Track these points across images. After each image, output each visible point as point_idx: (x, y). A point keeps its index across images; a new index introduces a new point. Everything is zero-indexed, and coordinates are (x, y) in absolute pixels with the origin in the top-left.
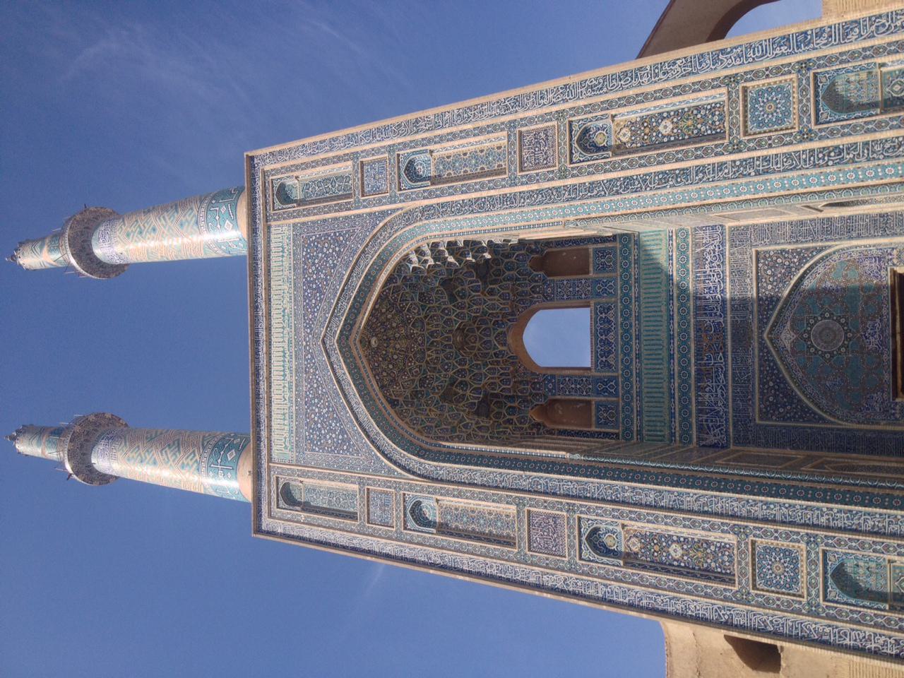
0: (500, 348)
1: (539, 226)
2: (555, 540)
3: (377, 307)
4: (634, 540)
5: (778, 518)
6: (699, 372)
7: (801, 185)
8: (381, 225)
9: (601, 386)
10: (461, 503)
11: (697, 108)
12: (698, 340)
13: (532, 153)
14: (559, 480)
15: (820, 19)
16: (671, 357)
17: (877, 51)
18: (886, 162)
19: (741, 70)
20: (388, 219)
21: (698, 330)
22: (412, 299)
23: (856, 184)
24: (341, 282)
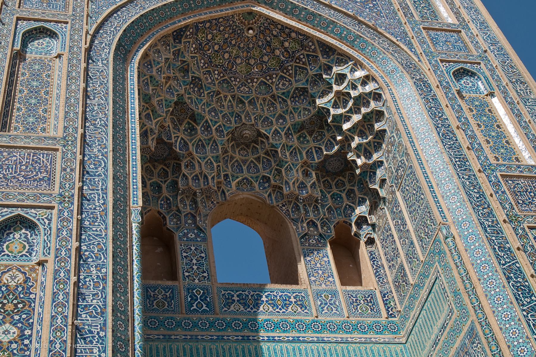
0: (234, 184)
2: (14, 177)
3: (293, 35)
4: (21, 278)
13: (527, 190)
20: (405, 48)
22: (296, 81)
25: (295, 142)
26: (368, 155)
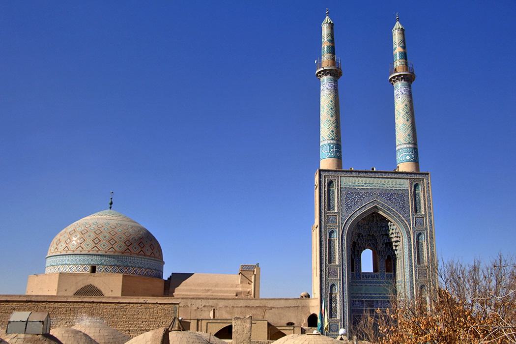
12: (370, 301)
16: (366, 294)
21: (373, 301)
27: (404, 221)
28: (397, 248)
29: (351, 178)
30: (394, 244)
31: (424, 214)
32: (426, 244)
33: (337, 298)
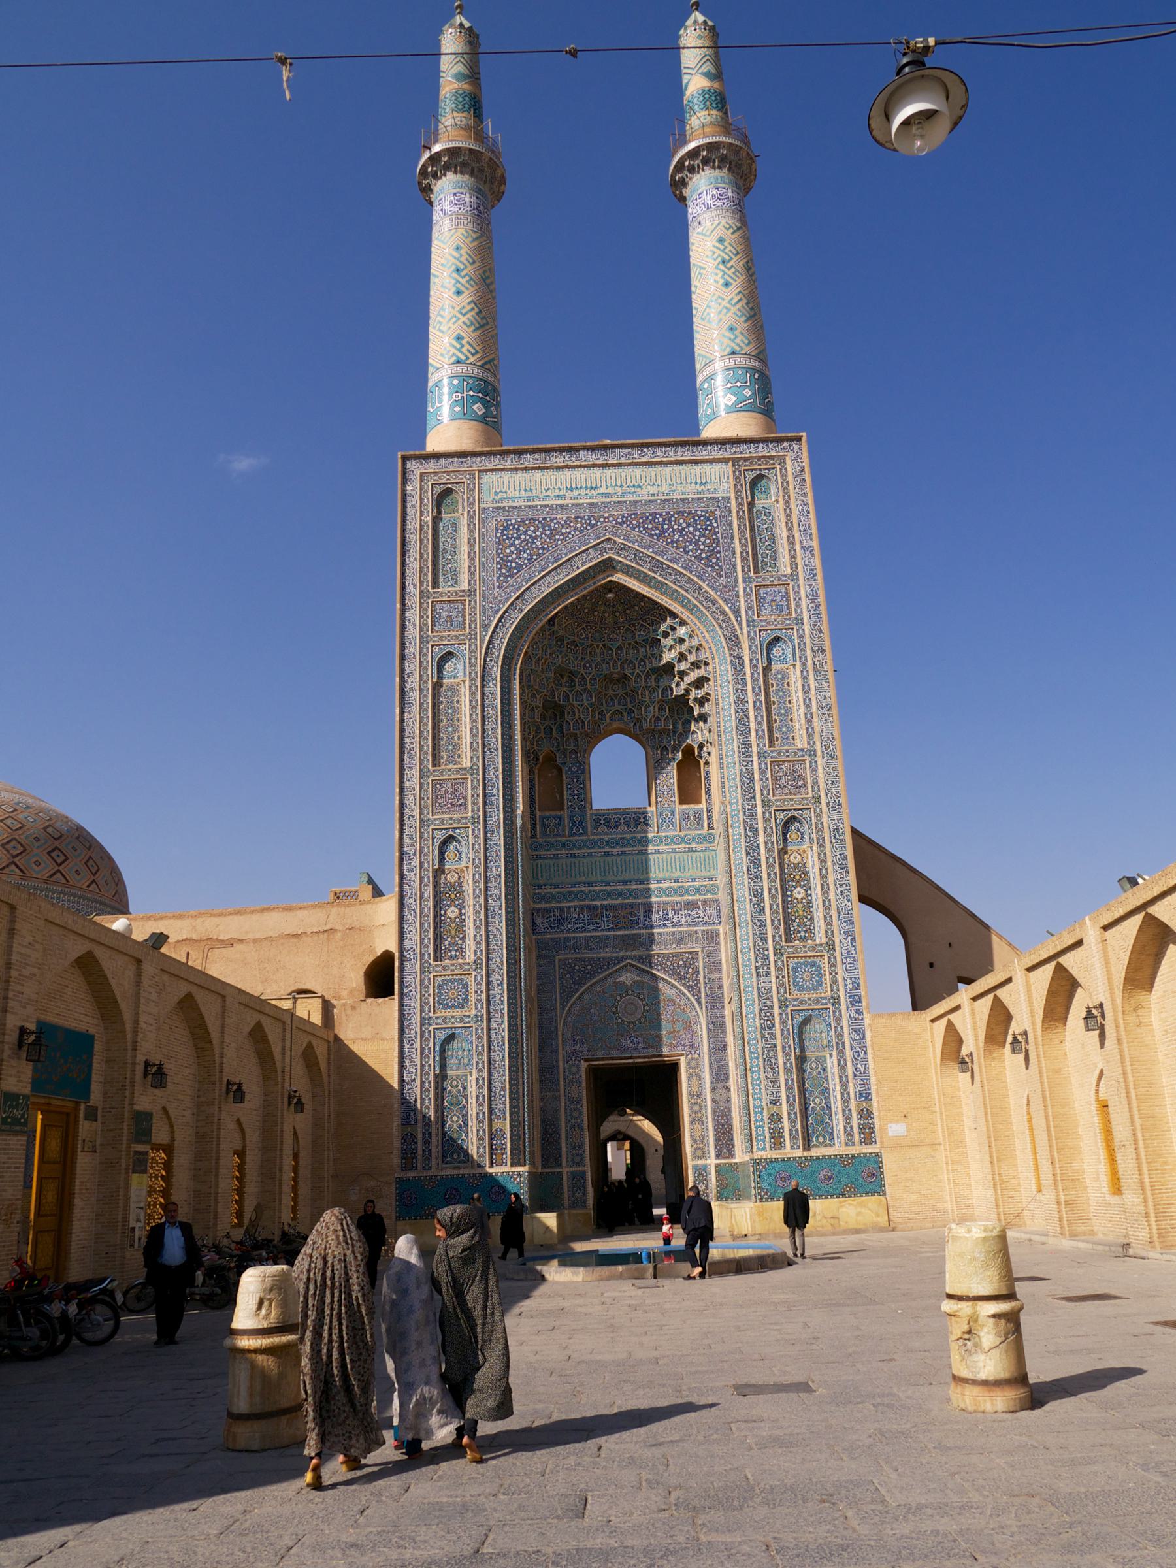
0: (608, 716)
1: (722, 778)
5: (491, 993)
6: (596, 908)
7: (747, 1000)
8: (727, 609)
9: (577, 819)
10: (465, 708)
11: (812, 918)
12: (623, 907)
14: (498, 807)
15: (869, 1012)
16: (608, 884)
17: (841, 1052)
18: (761, 1059)
19: (838, 954)
20: (732, 617)
21: (632, 906)
23: (746, 1039)
24: (670, 560)
25: (652, 683)
26: (701, 704)
27: (714, 602)
28: (706, 709)
29: (520, 473)
30: (693, 694)
31: (789, 571)
32: (799, 674)
33: (465, 887)
